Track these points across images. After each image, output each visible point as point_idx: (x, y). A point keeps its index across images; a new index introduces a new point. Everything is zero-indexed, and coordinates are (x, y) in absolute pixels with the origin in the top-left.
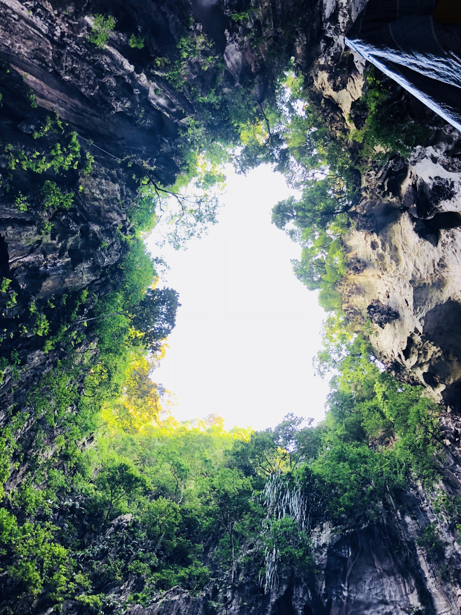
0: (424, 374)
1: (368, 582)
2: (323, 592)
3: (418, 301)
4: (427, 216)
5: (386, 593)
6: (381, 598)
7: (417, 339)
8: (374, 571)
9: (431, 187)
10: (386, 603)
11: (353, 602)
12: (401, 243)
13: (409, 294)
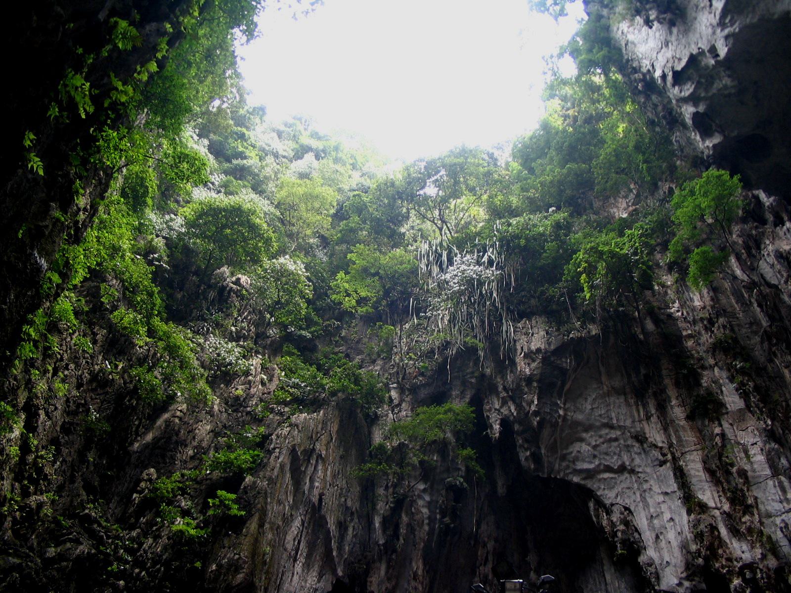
0: (695, 115)
1: (590, 400)
2: (533, 408)
5: (613, 415)
6: (605, 421)
8: (599, 387)
10: (612, 427)
11: (569, 422)
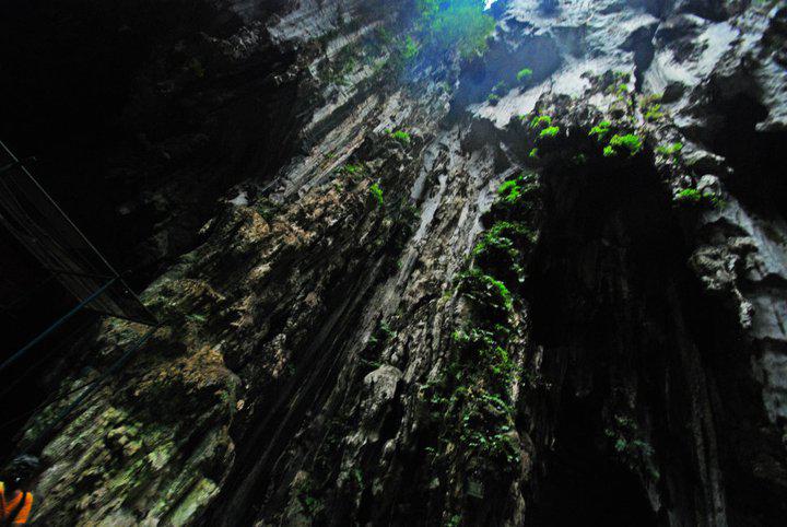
3: (563, 31)
7: (527, 32)
9: (693, 41)
13: (573, 23)
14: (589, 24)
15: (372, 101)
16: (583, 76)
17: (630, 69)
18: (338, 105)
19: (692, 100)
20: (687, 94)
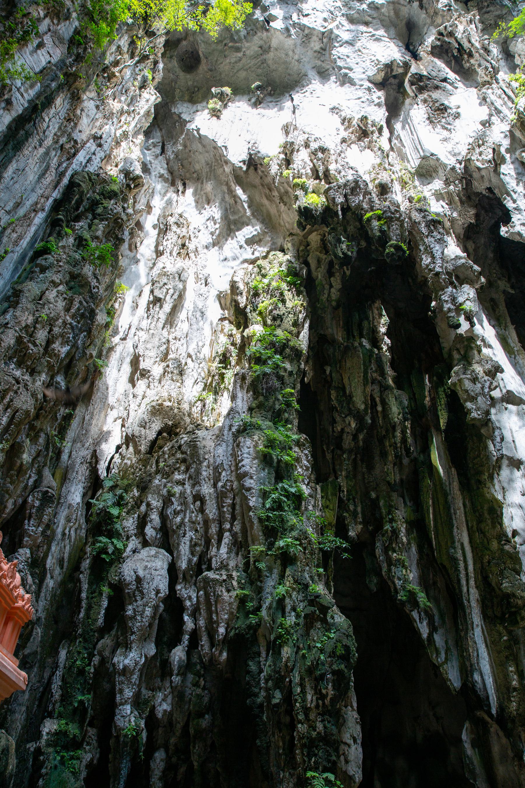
4: (412, 84)
12: (374, 32)
14: (336, 31)
15: (61, 103)
16: (334, 110)
17: (379, 115)
18: (14, 114)
19: (447, 183)
20: (441, 173)
